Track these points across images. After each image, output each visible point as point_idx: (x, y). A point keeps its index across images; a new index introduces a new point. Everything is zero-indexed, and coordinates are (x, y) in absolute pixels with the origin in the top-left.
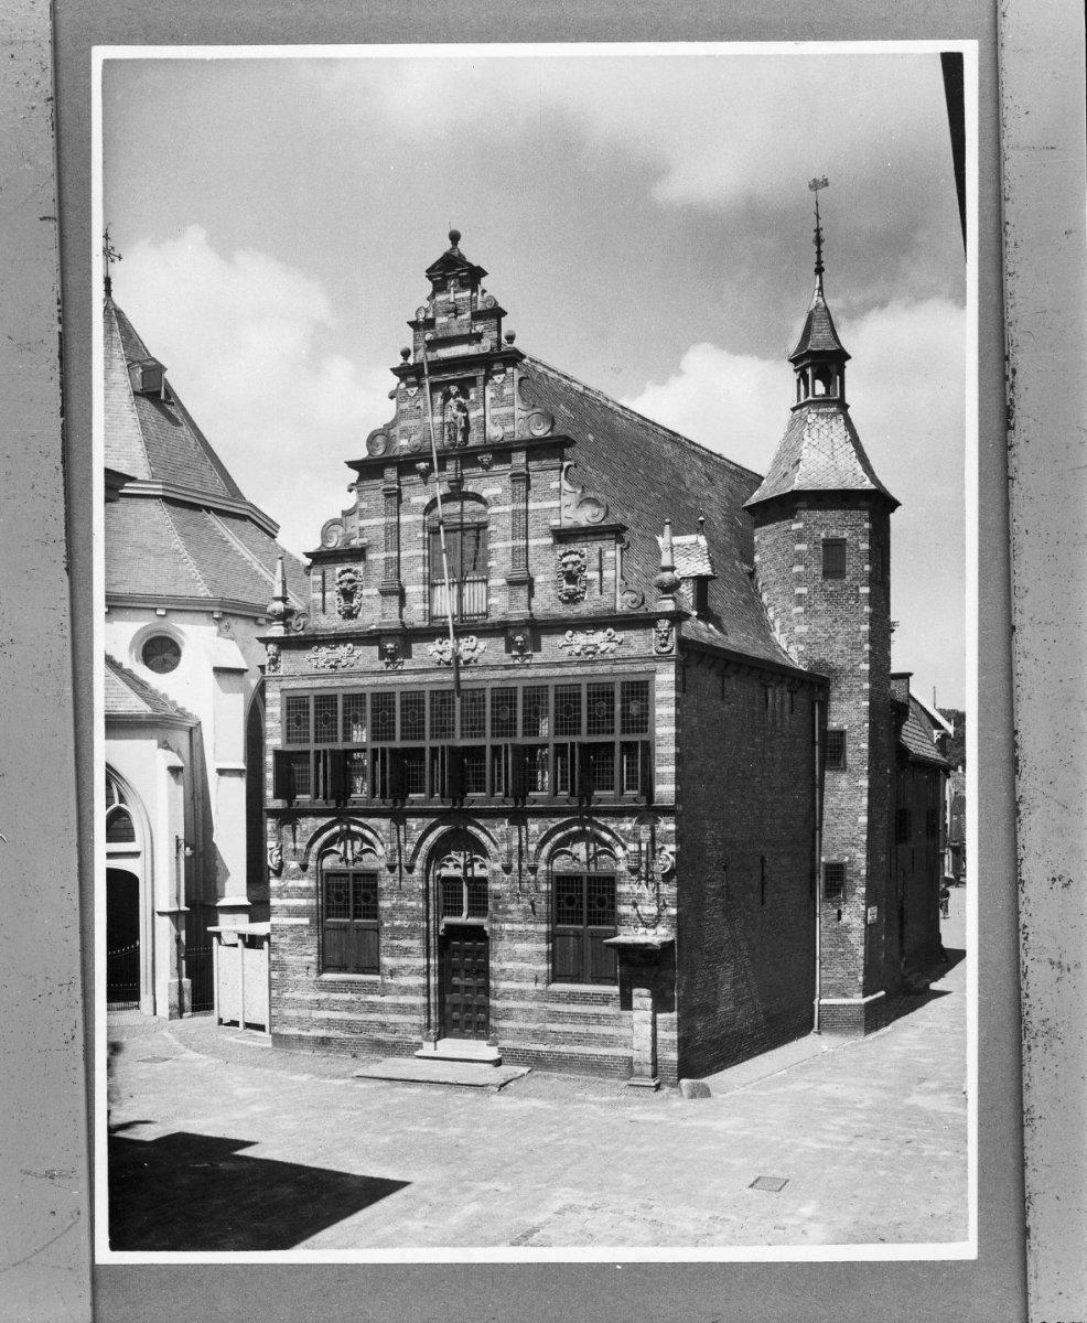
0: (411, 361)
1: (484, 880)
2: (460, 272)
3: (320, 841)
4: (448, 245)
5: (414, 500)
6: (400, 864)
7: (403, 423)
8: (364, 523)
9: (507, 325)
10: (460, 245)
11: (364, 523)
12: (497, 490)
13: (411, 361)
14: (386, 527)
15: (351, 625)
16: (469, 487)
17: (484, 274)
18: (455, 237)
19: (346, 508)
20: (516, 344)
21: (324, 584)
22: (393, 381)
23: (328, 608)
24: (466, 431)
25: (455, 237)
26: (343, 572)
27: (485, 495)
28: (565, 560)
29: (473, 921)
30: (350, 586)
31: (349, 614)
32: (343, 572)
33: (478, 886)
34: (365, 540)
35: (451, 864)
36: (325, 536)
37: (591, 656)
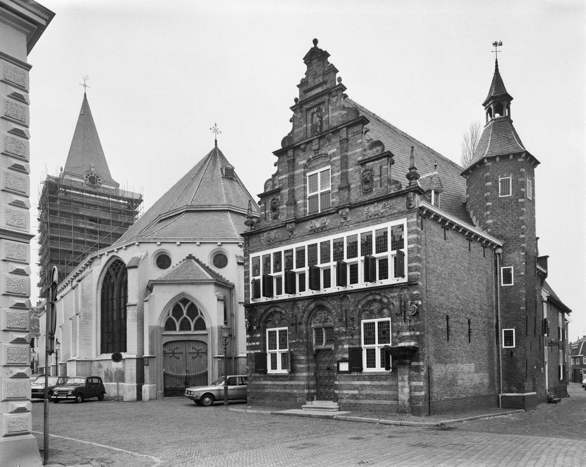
1: (332, 328)
2: (318, 55)
5: (301, 163)
8: (281, 178)
9: (338, 75)
11: (281, 178)
12: (335, 150)
17: (329, 55)
18: (315, 41)
19: (273, 174)
22: (291, 114)
23: (267, 217)
24: (321, 127)
25: (315, 41)
31: (275, 217)
32: (272, 200)
34: (281, 185)
35: (318, 322)
36: (265, 188)
37: (377, 216)
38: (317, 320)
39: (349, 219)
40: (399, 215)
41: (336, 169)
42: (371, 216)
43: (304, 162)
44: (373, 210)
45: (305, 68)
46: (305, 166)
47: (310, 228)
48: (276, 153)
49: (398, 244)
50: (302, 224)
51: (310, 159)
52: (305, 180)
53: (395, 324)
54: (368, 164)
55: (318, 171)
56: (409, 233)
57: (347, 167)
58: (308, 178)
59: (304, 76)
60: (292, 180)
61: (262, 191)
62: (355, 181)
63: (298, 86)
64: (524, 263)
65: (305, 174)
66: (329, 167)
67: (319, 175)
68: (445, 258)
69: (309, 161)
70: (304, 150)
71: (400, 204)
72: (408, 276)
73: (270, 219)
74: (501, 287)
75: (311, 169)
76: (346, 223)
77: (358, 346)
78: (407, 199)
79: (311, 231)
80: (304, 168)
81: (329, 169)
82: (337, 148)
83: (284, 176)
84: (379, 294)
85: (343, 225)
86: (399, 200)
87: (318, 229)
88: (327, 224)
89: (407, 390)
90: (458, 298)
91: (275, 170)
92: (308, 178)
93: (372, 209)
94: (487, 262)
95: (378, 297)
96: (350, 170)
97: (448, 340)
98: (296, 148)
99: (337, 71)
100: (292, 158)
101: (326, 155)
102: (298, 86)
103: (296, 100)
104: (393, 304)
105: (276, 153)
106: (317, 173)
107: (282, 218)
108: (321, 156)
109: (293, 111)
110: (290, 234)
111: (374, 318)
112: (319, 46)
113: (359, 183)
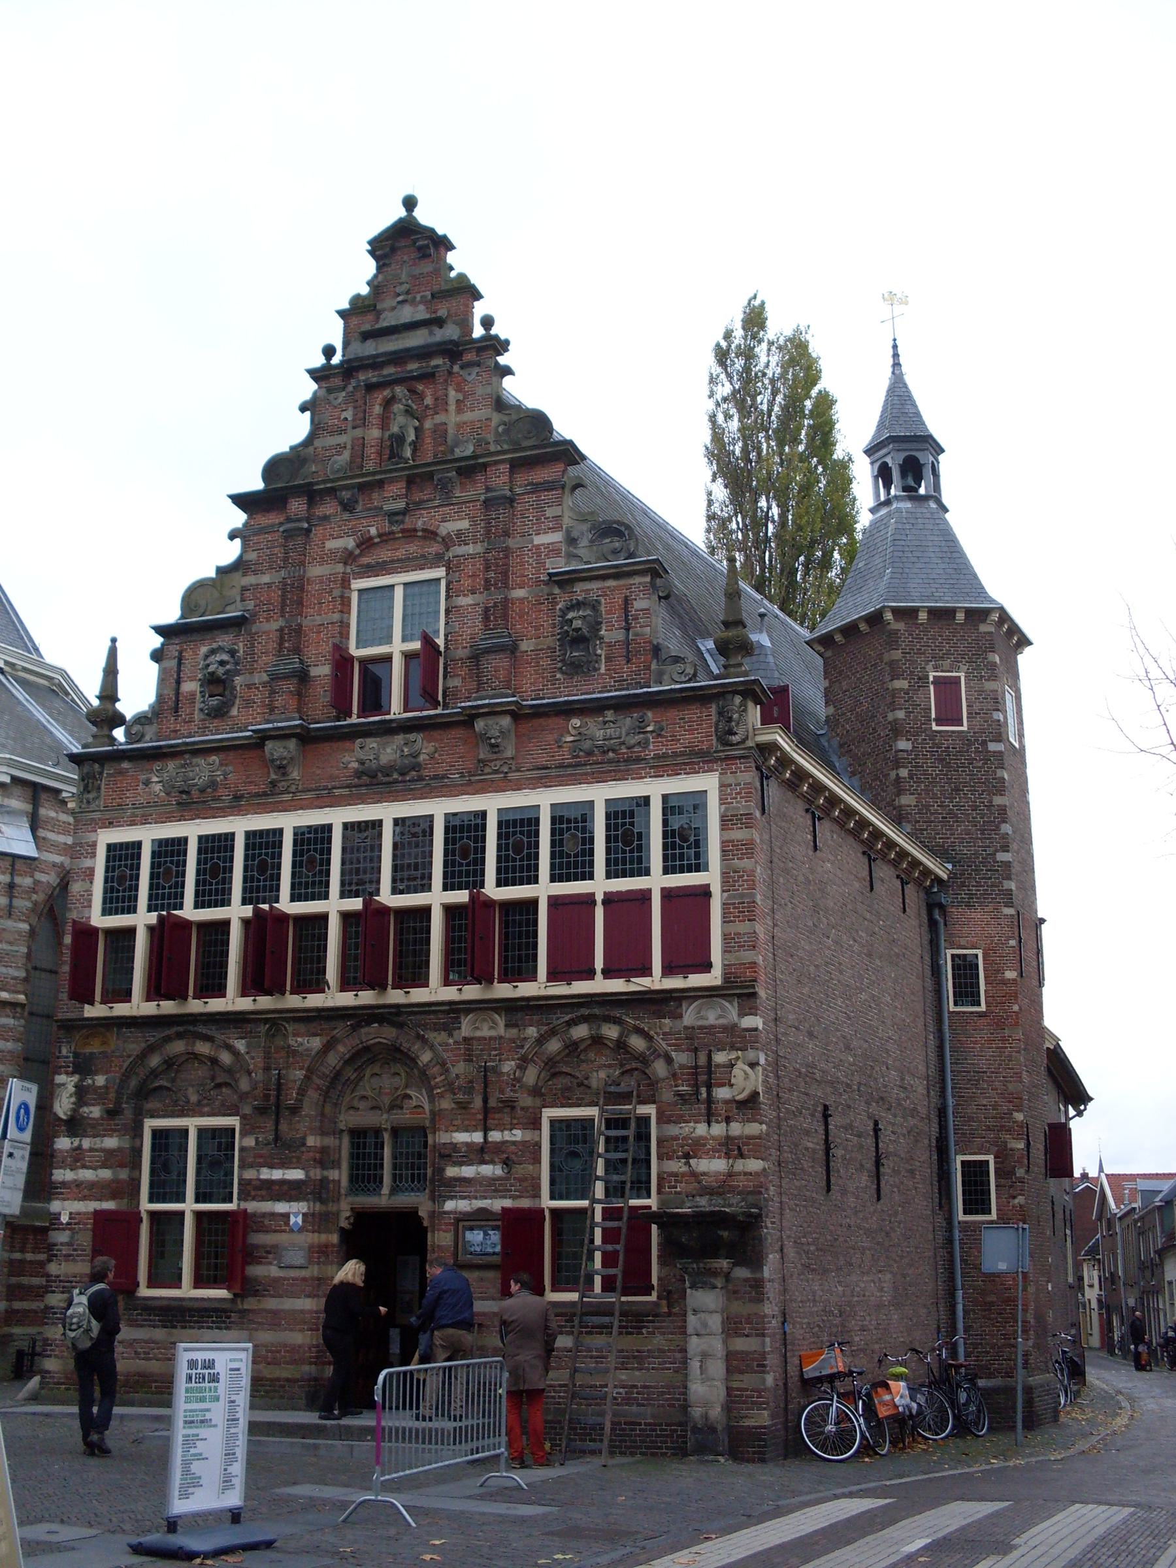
0: (336, 360)
3: (142, 1072)
4: (403, 213)
5: (331, 544)
7: (317, 443)
8: (250, 580)
9: (480, 310)
10: (418, 213)
11: (250, 580)
13: (336, 360)
16: (420, 521)
17: (450, 247)
18: (410, 203)
20: (493, 332)
21: (179, 671)
22: (309, 388)
25: (410, 203)
26: (213, 652)
28: (570, 615)
29: (405, 1200)
30: (221, 670)
34: (250, 605)
39: (509, 753)
40: (693, 760)
41: (467, 583)
42: (590, 753)
43: (350, 543)
44: (600, 734)
45: (369, 267)
46: (348, 557)
47: (355, 765)
48: (242, 500)
49: (684, 850)
50: (327, 746)
51: (371, 538)
52: (346, 603)
53: (673, 1130)
54: (579, 587)
57: (504, 582)
58: (355, 597)
59: (365, 290)
60: (294, 595)
61: (172, 614)
63: (342, 314)
64: (1013, 943)
65: (345, 583)
66: (440, 572)
67: (399, 593)
68: (816, 909)
69: (366, 544)
71: (697, 727)
73: (197, 716)
74: (949, 1012)
76: (498, 763)
77: (525, 1203)
78: (720, 714)
79: (359, 774)
80: (345, 564)
82: (472, 519)
83: (266, 579)
84: (617, 1021)
85: (487, 770)
86: (692, 713)
87: (387, 770)
88: (422, 758)
89: (717, 1368)
90: (848, 1048)
91: (232, 551)
92: (355, 597)
93: (597, 730)
94: (910, 931)
95: (611, 1032)
97: (829, 1190)
98: (312, 495)
99: (477, 296)
100: (306, 525)
101: (430, 535)
102: (342, 314)
103: (329, 351)
104: (669, 1060)
105: (242, 500)
106: (393, 586)
108: (410, 534)
109: (316, 379)
110: (273, 776)
112: (422, 216)
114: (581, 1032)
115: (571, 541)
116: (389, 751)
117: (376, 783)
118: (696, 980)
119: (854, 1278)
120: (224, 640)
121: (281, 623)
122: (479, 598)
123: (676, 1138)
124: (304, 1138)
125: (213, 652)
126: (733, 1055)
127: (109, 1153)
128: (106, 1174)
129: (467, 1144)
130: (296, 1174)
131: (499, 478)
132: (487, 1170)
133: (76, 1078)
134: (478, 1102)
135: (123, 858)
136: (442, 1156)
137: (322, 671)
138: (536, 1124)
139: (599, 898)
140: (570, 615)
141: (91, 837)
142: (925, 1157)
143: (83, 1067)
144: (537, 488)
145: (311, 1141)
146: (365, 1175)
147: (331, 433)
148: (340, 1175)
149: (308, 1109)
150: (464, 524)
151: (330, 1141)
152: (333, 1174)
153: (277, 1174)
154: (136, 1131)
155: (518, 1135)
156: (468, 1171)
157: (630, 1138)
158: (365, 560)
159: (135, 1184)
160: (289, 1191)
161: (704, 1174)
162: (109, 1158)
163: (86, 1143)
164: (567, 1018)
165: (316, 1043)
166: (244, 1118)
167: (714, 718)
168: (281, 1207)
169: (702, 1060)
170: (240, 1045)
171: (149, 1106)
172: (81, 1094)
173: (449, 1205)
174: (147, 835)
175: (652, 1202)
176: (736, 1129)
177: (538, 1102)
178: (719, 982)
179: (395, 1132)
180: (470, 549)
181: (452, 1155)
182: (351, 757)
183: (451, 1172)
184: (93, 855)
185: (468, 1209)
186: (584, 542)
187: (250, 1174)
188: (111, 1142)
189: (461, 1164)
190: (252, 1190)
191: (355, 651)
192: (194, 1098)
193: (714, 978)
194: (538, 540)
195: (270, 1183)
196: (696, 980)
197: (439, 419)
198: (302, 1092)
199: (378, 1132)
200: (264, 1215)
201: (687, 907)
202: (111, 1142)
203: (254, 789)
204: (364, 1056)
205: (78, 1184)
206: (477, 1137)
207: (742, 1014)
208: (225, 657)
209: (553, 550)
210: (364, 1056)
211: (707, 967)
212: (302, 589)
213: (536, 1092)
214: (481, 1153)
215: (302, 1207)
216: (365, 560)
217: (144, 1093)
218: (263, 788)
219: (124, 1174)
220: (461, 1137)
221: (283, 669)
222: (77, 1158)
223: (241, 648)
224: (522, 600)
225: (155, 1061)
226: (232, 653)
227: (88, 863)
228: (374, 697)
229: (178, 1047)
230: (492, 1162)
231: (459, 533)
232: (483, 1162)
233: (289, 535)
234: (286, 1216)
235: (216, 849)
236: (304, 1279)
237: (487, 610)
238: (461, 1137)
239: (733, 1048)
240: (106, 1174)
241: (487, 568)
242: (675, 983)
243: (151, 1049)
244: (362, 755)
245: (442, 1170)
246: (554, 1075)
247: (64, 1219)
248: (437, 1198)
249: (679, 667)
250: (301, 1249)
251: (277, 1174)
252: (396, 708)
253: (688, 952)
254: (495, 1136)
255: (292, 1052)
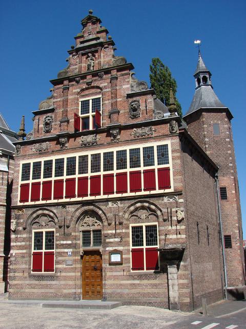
1: (100, 231)
3: (32, 218)
5: (74, 91)
6: (64, 226)
8: (55, 100)
11: (55, 100)
14: (63, 101)
15: (49, 136)
26: (47, 117)
27: (101, 86)
28: (132, 104)
33: (98, 233)
34: (55, 106)
38: (85, 223)
40: (165, 136)
46: (78, 93)
53: (162, 228)
55: (91, 98)
56: (173, 151)
62: (124, 110)
65: (78, 99)
66: (100, 96)
67: (91, 101)
70: (78, 82)
71: (165, 128)
72: (174, 187)
75: (83, 96)
81: (100, 98)
88: (97, 140)
89: (176, 288)
92: (80, 103)
96: (118, 100)
101: (98, 87)
107: (54, 133)
108: (93, 87)
111: (142, 222)
113: (128, 110)
114: (139, 205)
115: (132, 87)
116: (90, 138)
117: (86, 146)
118: (167, 191)
119: (205, 264)
120: (49, 114)
121: (63, 110)
122: (110, 101)
123: (163, 230)
124: (71, 233)
125: (47, 117)
126: (177, 209)
127: (24, 238)
128: (23, 243)
129: (111, 233)
130: (69, 242)
131: (114, 73)
132: (117, 240)
133: (16, 220)
134: (114, 223)
135: (26, 167)
136: (105, 237)
137: (72, 121)
138: (128, 228)
139: (142, 172)
140: (132, 104)
141: (18, 163)
142: (217, 234)
143: (18, 218)
144: (123, 75)
145: (73, 234)
146: (86, 242)
147: (74, 65)
148: (80, 242)
149: (72, 226)
150: (106, 84)
151: (77, 234)
152: (78, 242)
153: (65, 242)
154: (30, 232)
155: (124, 231)
156: (112, 240)
157: (151, 230)
158: (82, 94)
159: (30, 246)
160: (68, 246)
161: (171, 239)
162: (24, 240)
163: (19, 236)
164: (136, 201)
165: (73, 210)
166: (56, 229)
167: (169, 127)
168: (66, 250)
169: (169, 210)
170: (55, 211)
171: (33, 226)
172: (17, 224)
173: (107, 249)
174: (31, 161)
175: (158, 246)
176: (178, 227)
177: (128, 222)
178: (173, 191)
179: (93, 231)
180: (108, 90)
181: (107, 236)
182: (80, 140)
183: (108, 240)
184: (19, 166)
185: (112, 250)
186: (135, 87)
187: (58, 242)
188: (24, 236)
189: (110, 238)
190: (59, 246)
191: (80, 115)
192: (44, 224)
193: (171, 190)
194: (124, 87)
195: (63, 244)
196: (167, 191)
197: (99, 60)
198: (70, 221)
199: (89, 231)
200: (62, 252)
201: (164, 173)
202: (24, 236)
203: (57, 149)
204: (85, 213)
205: (17, 246)
206: (114, 232)
207: (179, 199)
208: (50, 118)
209: (128, 88)
210: (85, 213)
211: (170, 188)
212: (67, 101)
213: (128, 220)
214: (115, 236)
215: (71, 250)
216: (82, 94)
217: (33, 223)
218: (59, 149)
219: (28, 243)
220: (110, 232)
221: (63, 120)
222: (17, 240)
223: (53, 116)
224: (120, 101)
225: (35, 215)
226: (51, 117)
227: (17, 169)
228: (86, 125)
229: (40, 212)
230: (118, 238)
231: (105, 86)
232: (115, 238)
233: (64, 89)
234: (67, 252)
235: (48, 164)
236: (72, 268)
237: (112, 104)
238: (110, 232)
239: (177, 207)
240: (23, 243)
241: (112, 94)
242: (162, 191)
243: (34, 212)
244: (83, 140)
245: (105, 240)
246: (132, 216)
247: (14, 255)
248: (105, 247)
249: (160, 115)
250: (71, 260)
251: (65, 242)
252: (91, 128)
253: (165, 184)
254: (118, 231)
255: (67, 212)
